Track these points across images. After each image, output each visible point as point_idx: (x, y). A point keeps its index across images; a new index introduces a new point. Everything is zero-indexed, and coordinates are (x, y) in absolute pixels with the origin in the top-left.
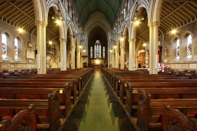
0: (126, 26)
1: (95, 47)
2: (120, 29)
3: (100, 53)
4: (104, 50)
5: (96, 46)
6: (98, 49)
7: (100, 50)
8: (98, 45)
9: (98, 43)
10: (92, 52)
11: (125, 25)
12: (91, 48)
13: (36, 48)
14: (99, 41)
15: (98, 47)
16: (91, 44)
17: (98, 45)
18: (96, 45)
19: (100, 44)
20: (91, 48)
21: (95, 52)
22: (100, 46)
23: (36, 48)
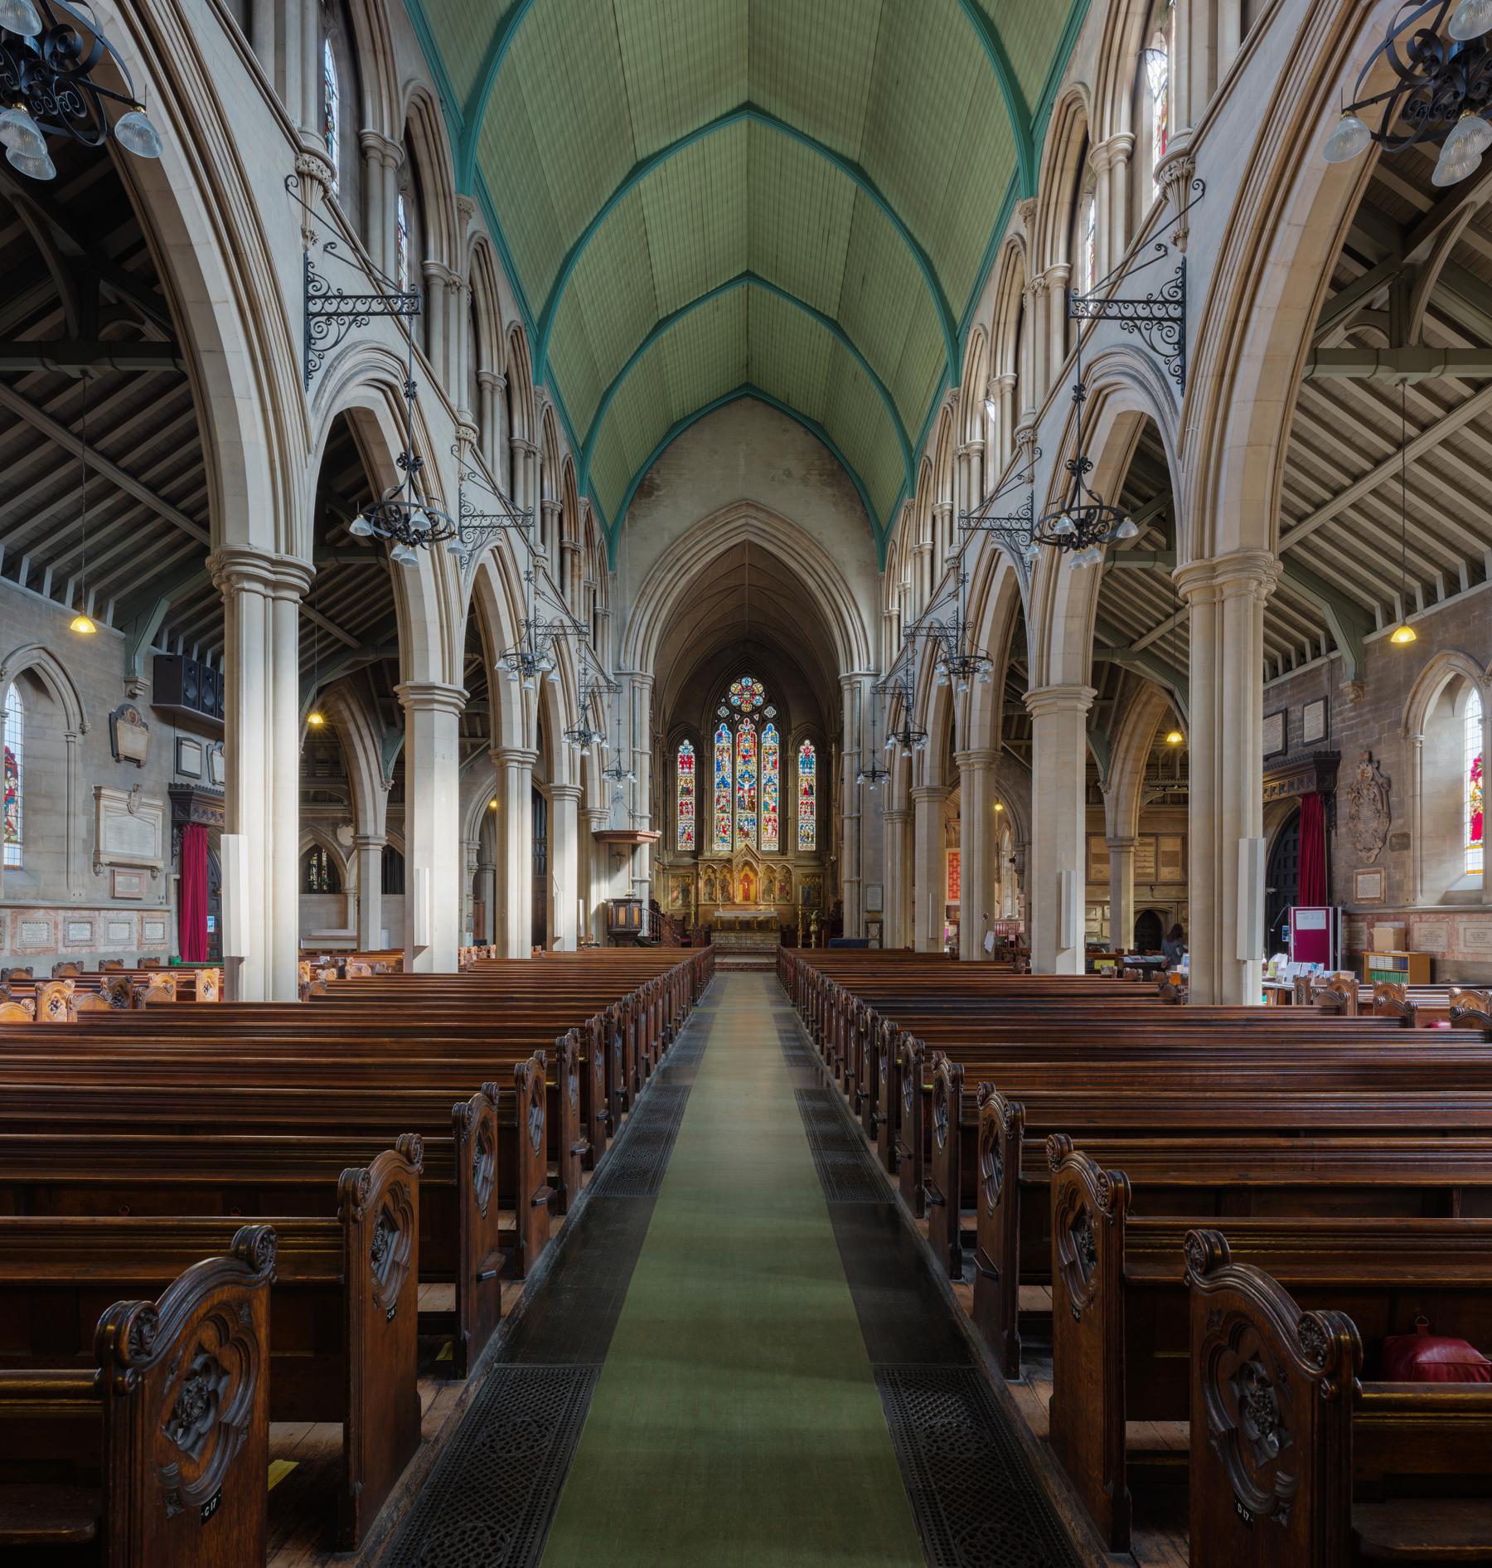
0: (1006, 560)
1: (723, 740)
2: (951, 586)
3: (771, 798)
4: (806, 775)
5: (723, 729)
6: (753, 767)
7: (771, 773)
8: (747, 727)
9: (746, 708)
10: (687, 792)
11: (995, 555)
12: (686, 749)
13: (178, 770)
14: (759, 688)
15: (746, 744)
16: (686, 715)
17: (747, 727)
18: (733, 728)
19: (770, 712)
20: (686, 749)
21: (721, 794)
22: (770, 739)
23: (178, 770)
